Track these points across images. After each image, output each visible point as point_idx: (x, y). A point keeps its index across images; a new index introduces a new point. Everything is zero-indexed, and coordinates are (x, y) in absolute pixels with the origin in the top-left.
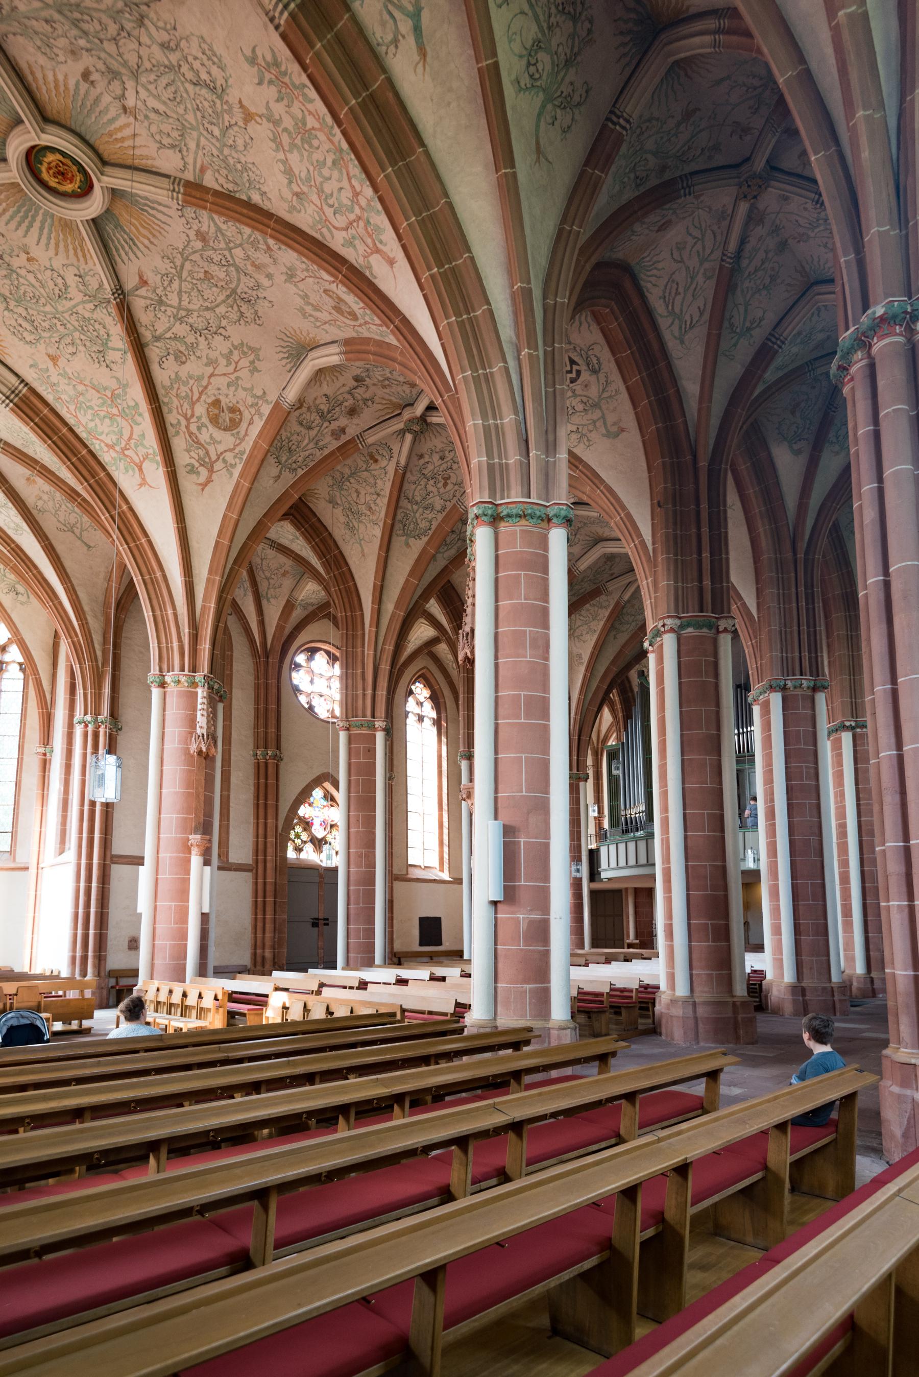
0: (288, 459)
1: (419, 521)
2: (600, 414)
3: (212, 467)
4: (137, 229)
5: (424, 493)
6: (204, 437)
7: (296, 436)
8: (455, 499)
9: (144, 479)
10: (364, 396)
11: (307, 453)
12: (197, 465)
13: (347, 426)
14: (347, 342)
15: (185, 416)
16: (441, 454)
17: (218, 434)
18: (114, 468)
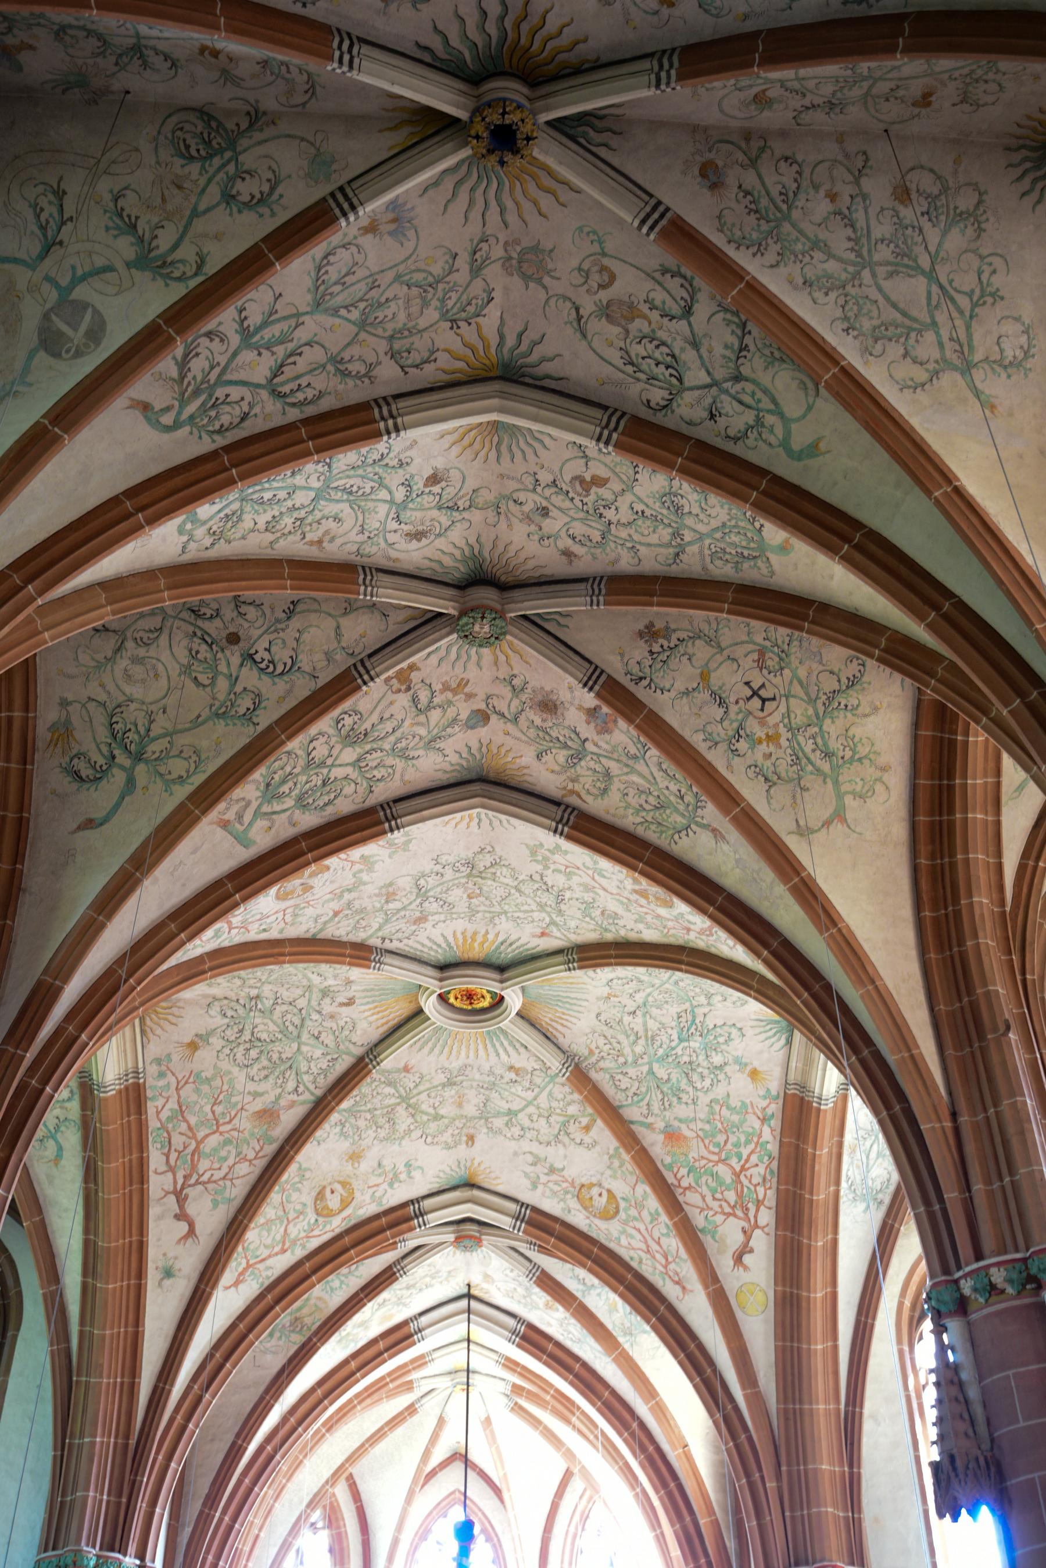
0: (677, 810)
1: (714, 523)
4: (482, 944)
5: (644, 525)
7: (629, 799)
10: (510, 695)
11: (659, 775)
13: (580, 708)
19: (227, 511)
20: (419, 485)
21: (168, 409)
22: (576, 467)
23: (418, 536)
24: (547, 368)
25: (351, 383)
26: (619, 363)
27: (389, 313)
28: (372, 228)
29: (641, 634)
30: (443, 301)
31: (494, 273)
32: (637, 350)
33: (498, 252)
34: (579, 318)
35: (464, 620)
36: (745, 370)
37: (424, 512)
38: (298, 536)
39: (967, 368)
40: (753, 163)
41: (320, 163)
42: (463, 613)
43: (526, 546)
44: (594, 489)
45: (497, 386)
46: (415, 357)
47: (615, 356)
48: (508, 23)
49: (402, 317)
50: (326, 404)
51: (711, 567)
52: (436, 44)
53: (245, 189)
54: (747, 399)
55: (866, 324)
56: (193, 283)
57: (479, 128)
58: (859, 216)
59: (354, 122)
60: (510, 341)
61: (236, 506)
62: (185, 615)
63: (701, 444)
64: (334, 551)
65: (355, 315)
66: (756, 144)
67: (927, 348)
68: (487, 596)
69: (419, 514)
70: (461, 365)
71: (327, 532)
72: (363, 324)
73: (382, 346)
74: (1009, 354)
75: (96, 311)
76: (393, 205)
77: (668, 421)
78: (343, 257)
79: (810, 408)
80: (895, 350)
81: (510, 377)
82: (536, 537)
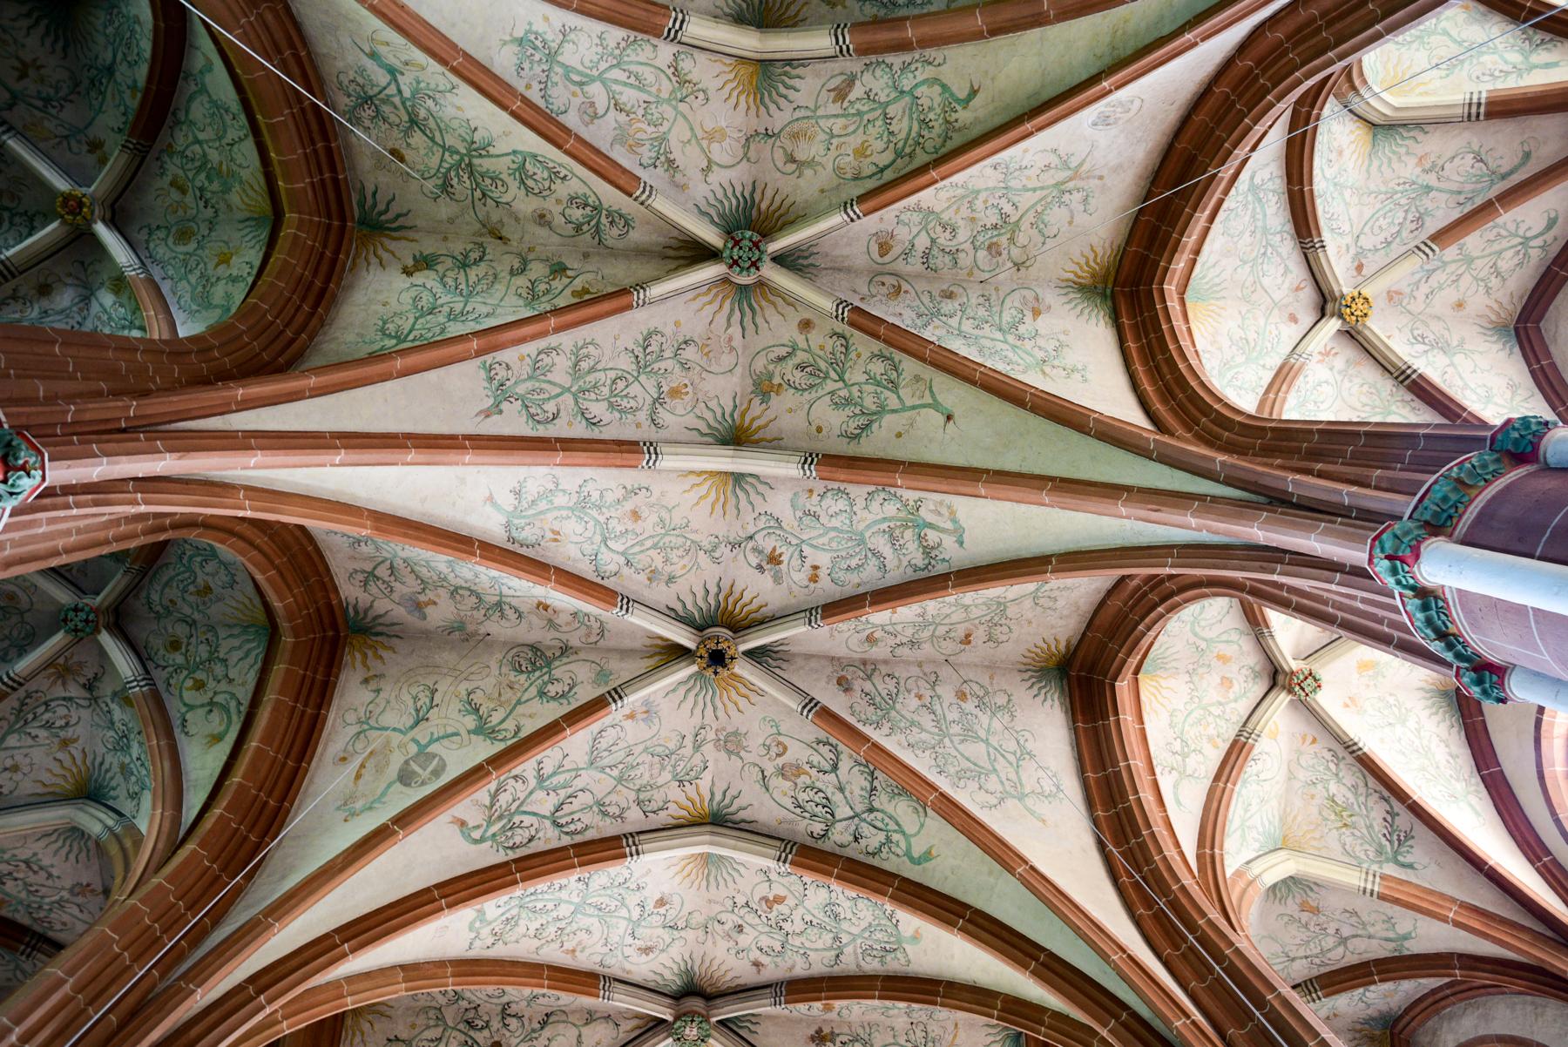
1: (864, 924)
5: (812, 933)
16: (734, 934)
19: (508, 915)
20: (650, 906)
21: (478, 827)
22: (763, 890)
23: (647, 950)
24: (742, 815)
25: (608, 820)
26: (791, 807)
27: (638, 773)
28: (631, 716)
29: (813, 1039)
30: (674, 767)
31: (708, 749)
32: (803, 797)
33: (711, 736)
34: (764, 778)
35: (678, 1024)
36: (876, 804)
37: (652, 931)
38: (556, 945)
39: (1021, 797)
40: (869, 677)
41: (602, 675)
42: (677, 1018)
43: (728, 961)
44: (776, 906)
45: (708, 828)
46: (653, 806)
47: (788, 802)
48: (721, 598)
49: (646, 777)
50: (590, 835)
51: (862, 963)
52: (679, 607)
53: (552, 689)
54: (879, 824)
55: (952, 770)
56: (509, 743)
57: (703, 652)
58: (937, 707)
59: (625, 653)
60: (718, 797)
61: (515, 912)
62: (461, 1026)
63: (849, 860)
64: (584, 961)
65: (615, 773)
66: (870, 668)
67: (992, 783)
68: (696, 1004)
69: (648, 931)
70: (685, 813)
71: (580, 943)
72: (620, 780)
73: (632, 796)
74: (1047, 789)
75: (441, 759)
76: (646, 702)
77: (826, 846)
78: (611, 735)
79: (922, 826)
80: (973, 785)
81: (718, 821)
82: (733, 952)
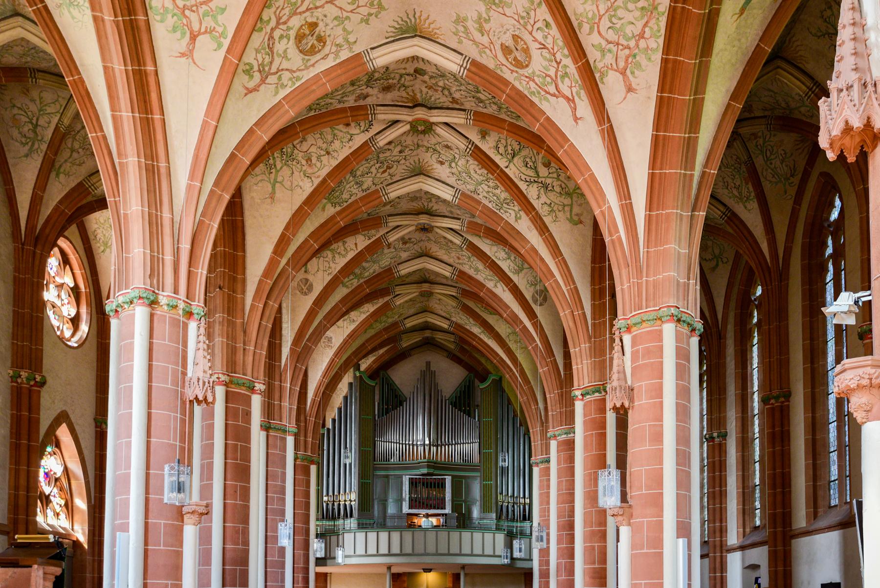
2: (570, 203)
3: (267, 77)
6: (279, 47)
8: (381, 186)
9: (191, 51)
12: (256, 68)
14: (474, 63)
15: (279, 19)
17: (293, 52)
18: (158, 18)
22: (391, 171)
